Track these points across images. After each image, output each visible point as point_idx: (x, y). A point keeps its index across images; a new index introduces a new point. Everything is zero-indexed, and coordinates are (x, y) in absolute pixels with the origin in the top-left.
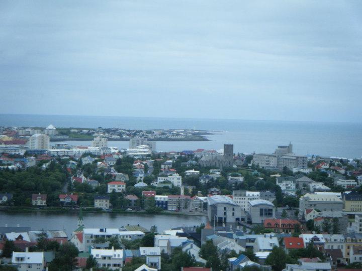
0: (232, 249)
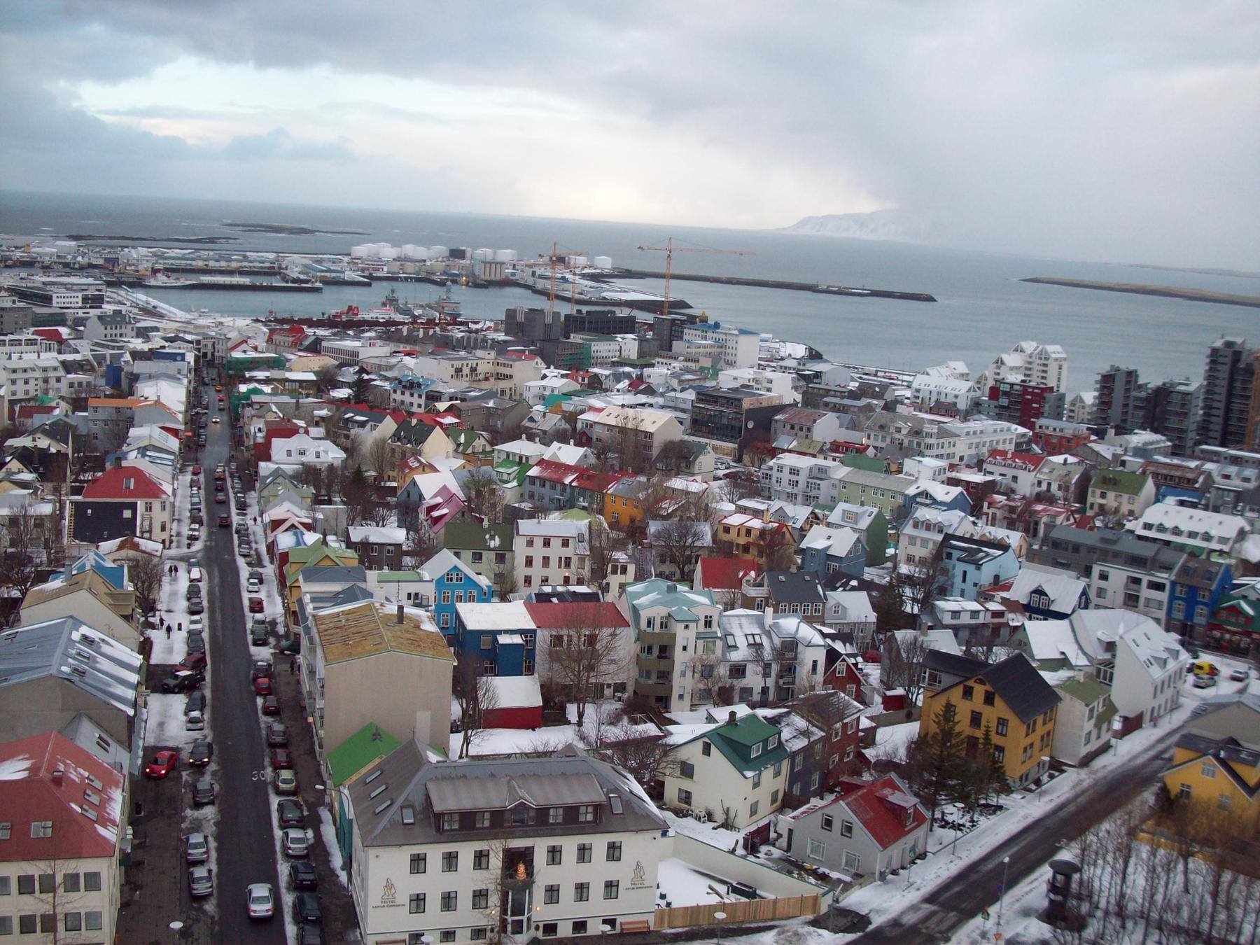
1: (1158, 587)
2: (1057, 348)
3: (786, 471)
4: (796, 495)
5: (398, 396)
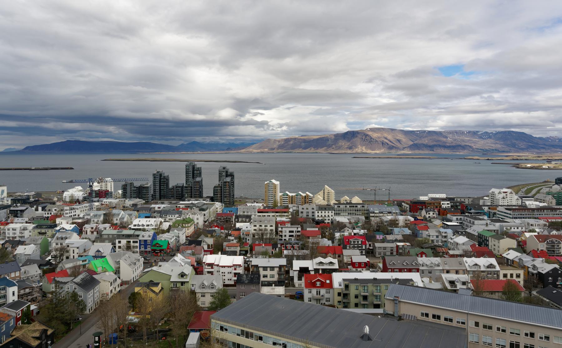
1: (137, 242)
3: (11, 230)
4: (16, 237)
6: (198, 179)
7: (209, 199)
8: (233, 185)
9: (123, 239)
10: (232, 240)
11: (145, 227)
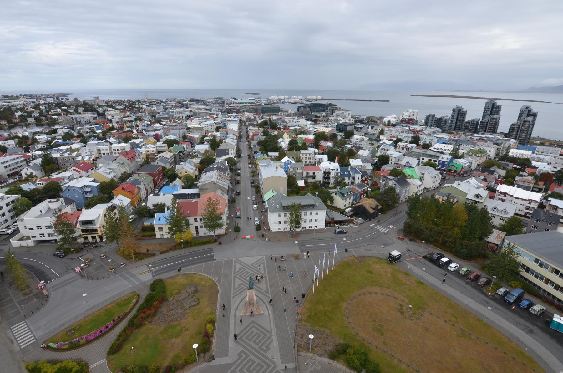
0: (87, 131)
1: (436, 161)
2: (417, 110)
5: (278, 126)
6: (496, 116)
7: (503, 135)
8: (533, 124)
9: (426, 157)
10: (525, 176)
11: (443, 151)
